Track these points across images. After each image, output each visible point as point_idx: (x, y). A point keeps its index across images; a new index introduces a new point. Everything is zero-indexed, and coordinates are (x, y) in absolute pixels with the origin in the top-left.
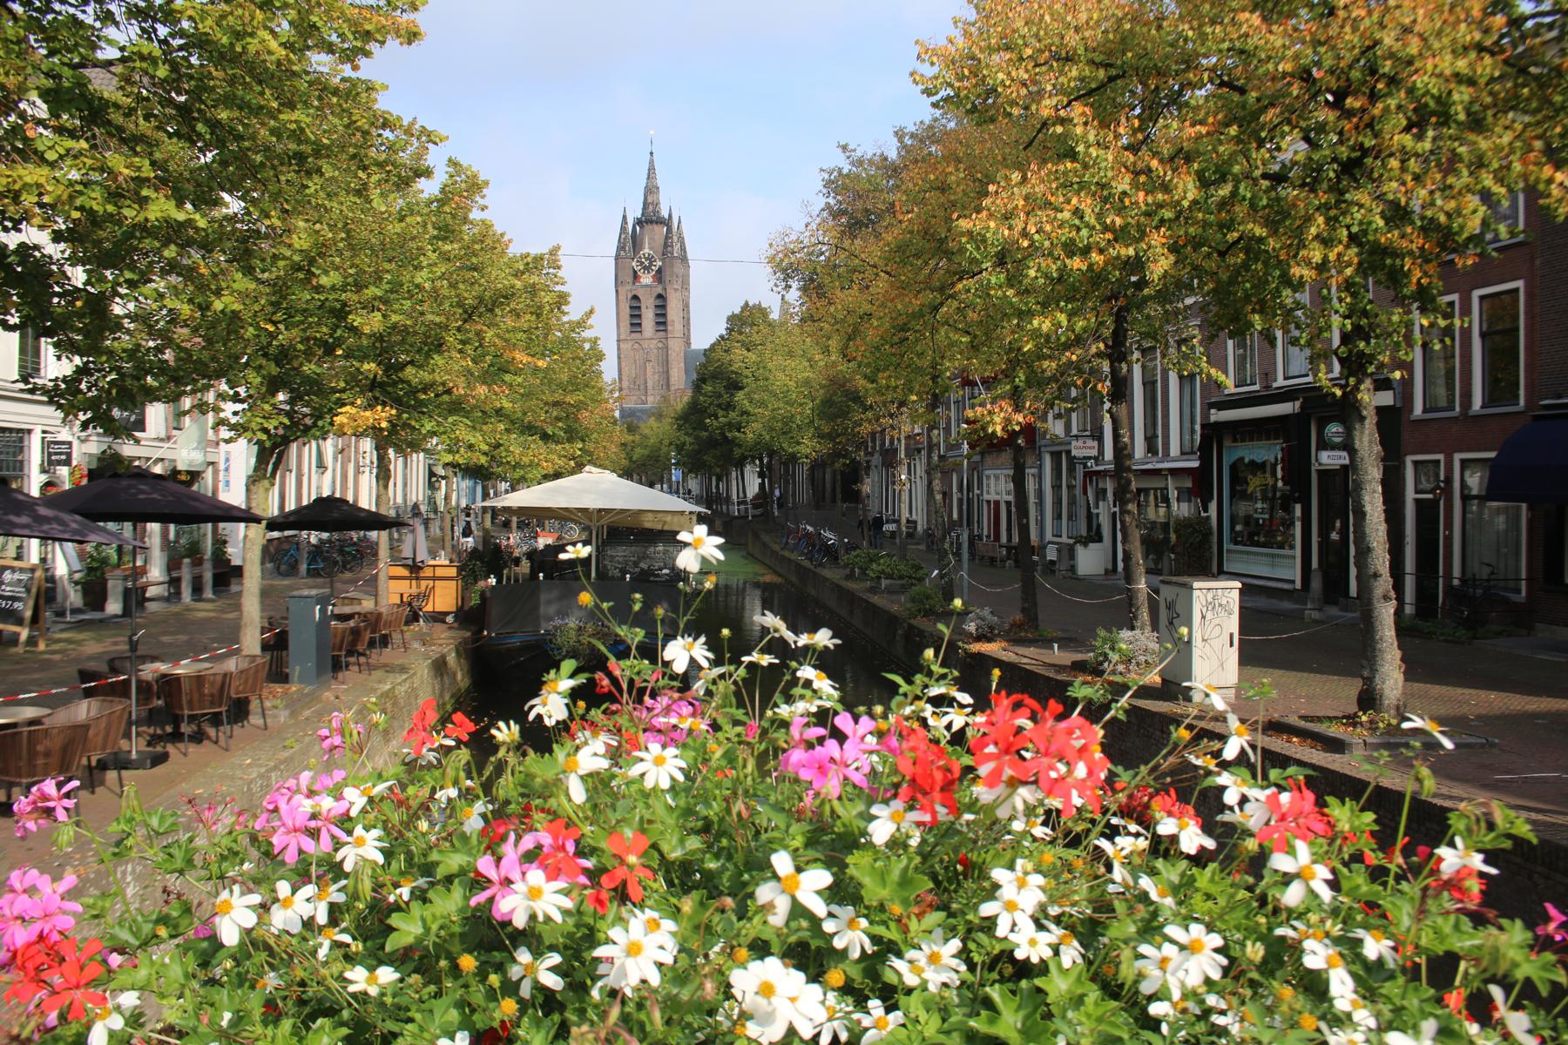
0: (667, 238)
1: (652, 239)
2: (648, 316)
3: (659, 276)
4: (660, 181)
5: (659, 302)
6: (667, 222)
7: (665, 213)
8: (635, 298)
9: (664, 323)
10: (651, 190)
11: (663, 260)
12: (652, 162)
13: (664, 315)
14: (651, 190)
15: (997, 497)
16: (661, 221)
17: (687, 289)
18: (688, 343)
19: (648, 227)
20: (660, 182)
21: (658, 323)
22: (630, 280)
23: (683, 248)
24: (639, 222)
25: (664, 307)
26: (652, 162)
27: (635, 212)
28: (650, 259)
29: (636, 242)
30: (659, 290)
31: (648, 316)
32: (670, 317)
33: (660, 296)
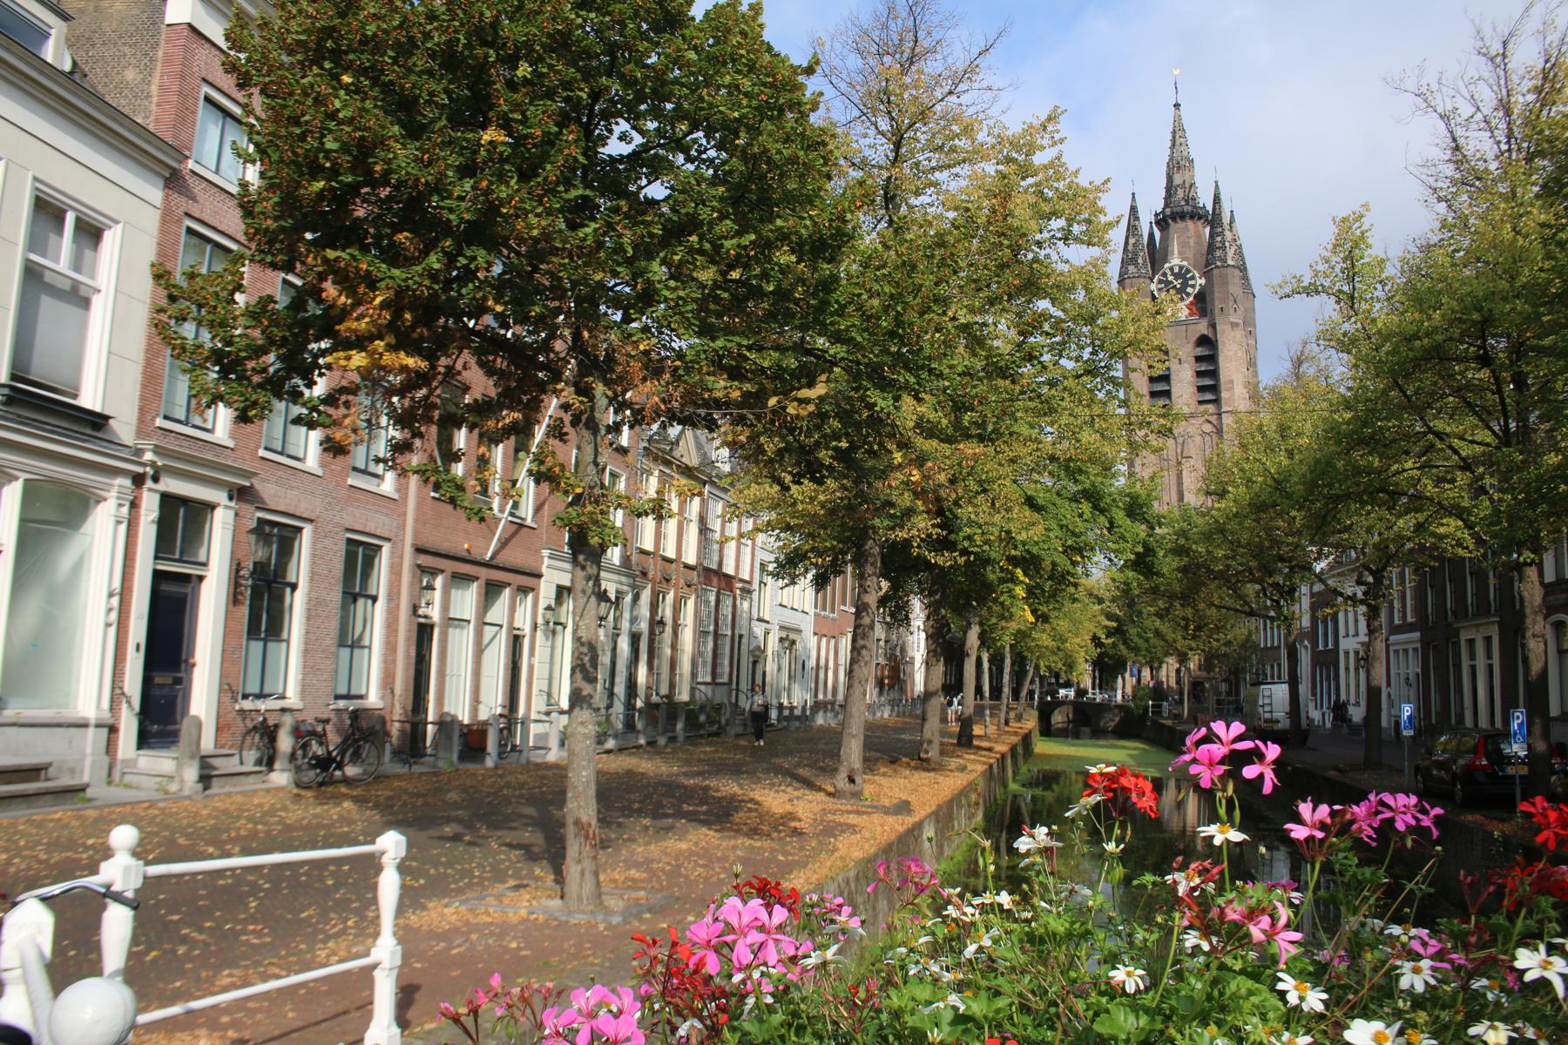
0: (1211, 247)
1: (1183, 245)
3: (1202, 304)
4: (1196, 148)
5: (1200, 351)
6: (1213, 220)
7: (1205, 200)
9: (1214, 389)
11: (1207, 274)
13: (1214, 374)
14: (1178, 164)
16: (1197, 215)
19: (1176, 227)
21: (1201, 389)
23: (1239, 252)
24: (1162, 222)
25: (1212, 359)
27: (1152, 204)
28: (1182, 274)
29: (1157, 256)
30: (1202, 328)
32: (1224, 376)
33: (1203, 341)
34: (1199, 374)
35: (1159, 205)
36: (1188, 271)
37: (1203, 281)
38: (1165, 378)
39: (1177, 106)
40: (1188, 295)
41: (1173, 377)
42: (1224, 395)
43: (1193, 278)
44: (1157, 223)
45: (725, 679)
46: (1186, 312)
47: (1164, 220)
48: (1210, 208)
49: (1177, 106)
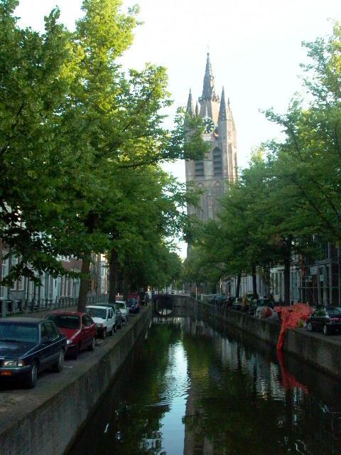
4: (213, 72)
10: (207, 80)
12: (208, 60)
14: (207, 80)
25: (220, 156)
26: (208, 60)
35: (200, 94)
39: (208, 54)
44: (200, 101)
45: (23, 289)
46: (210, 137)
47: (202, 100)
49: (208, 54)
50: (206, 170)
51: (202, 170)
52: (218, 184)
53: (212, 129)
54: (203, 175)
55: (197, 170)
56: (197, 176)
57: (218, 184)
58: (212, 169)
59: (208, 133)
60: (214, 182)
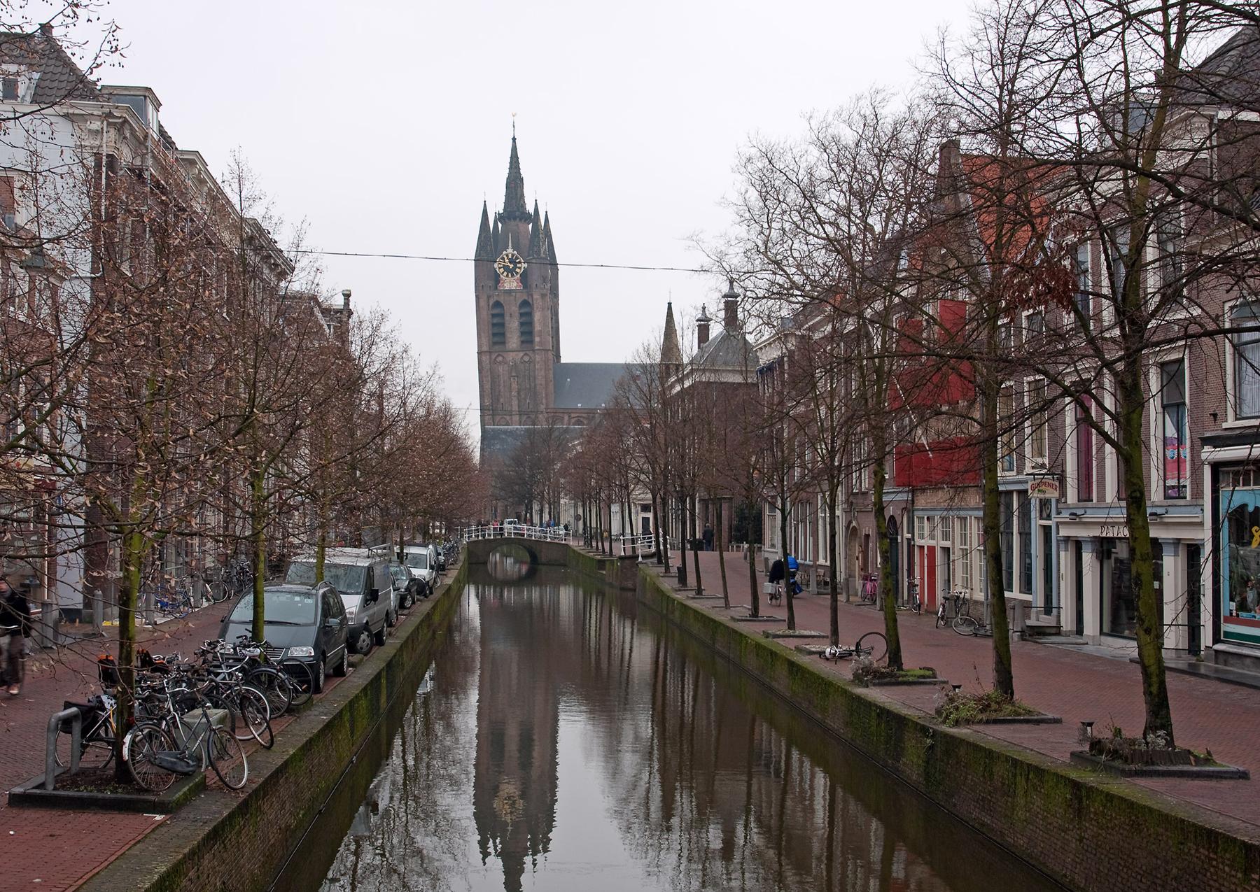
2: (513, 325)
7: (530, 208)
8: (498, 304)
10: (515, 183)
12: (514, 149)
14: (515, 183)
15: (932, 543)
16: (526, 217)
17: (556, 295)
18: (558, 356)
20: (524, 172)
21: (522, 333)
22: (491, 283)
24: (500, 218)
26: (514, 149)
27: (497, 205)
31: (513, 325)
33: (525, 304)
34: (522, 324)
36: (517, 258)
37: (526, 265)
38: (502, 325)
39: (514, 139)
40: (517, 273)
41: (507, 325)
42: (537, 339)
43: (520, 262)
46: (515, 284)
48: (532, 211)
49: (514, 139)
50: (508, 335)
51: (503, 334)
52: (526, 359)
53: (518, 270)
54: (504, 343)
55: (494, 335)
56: (495, 343)
57: (526, 359)
58: (519, 334)
59: (513, 276)
60: (521, 354)
